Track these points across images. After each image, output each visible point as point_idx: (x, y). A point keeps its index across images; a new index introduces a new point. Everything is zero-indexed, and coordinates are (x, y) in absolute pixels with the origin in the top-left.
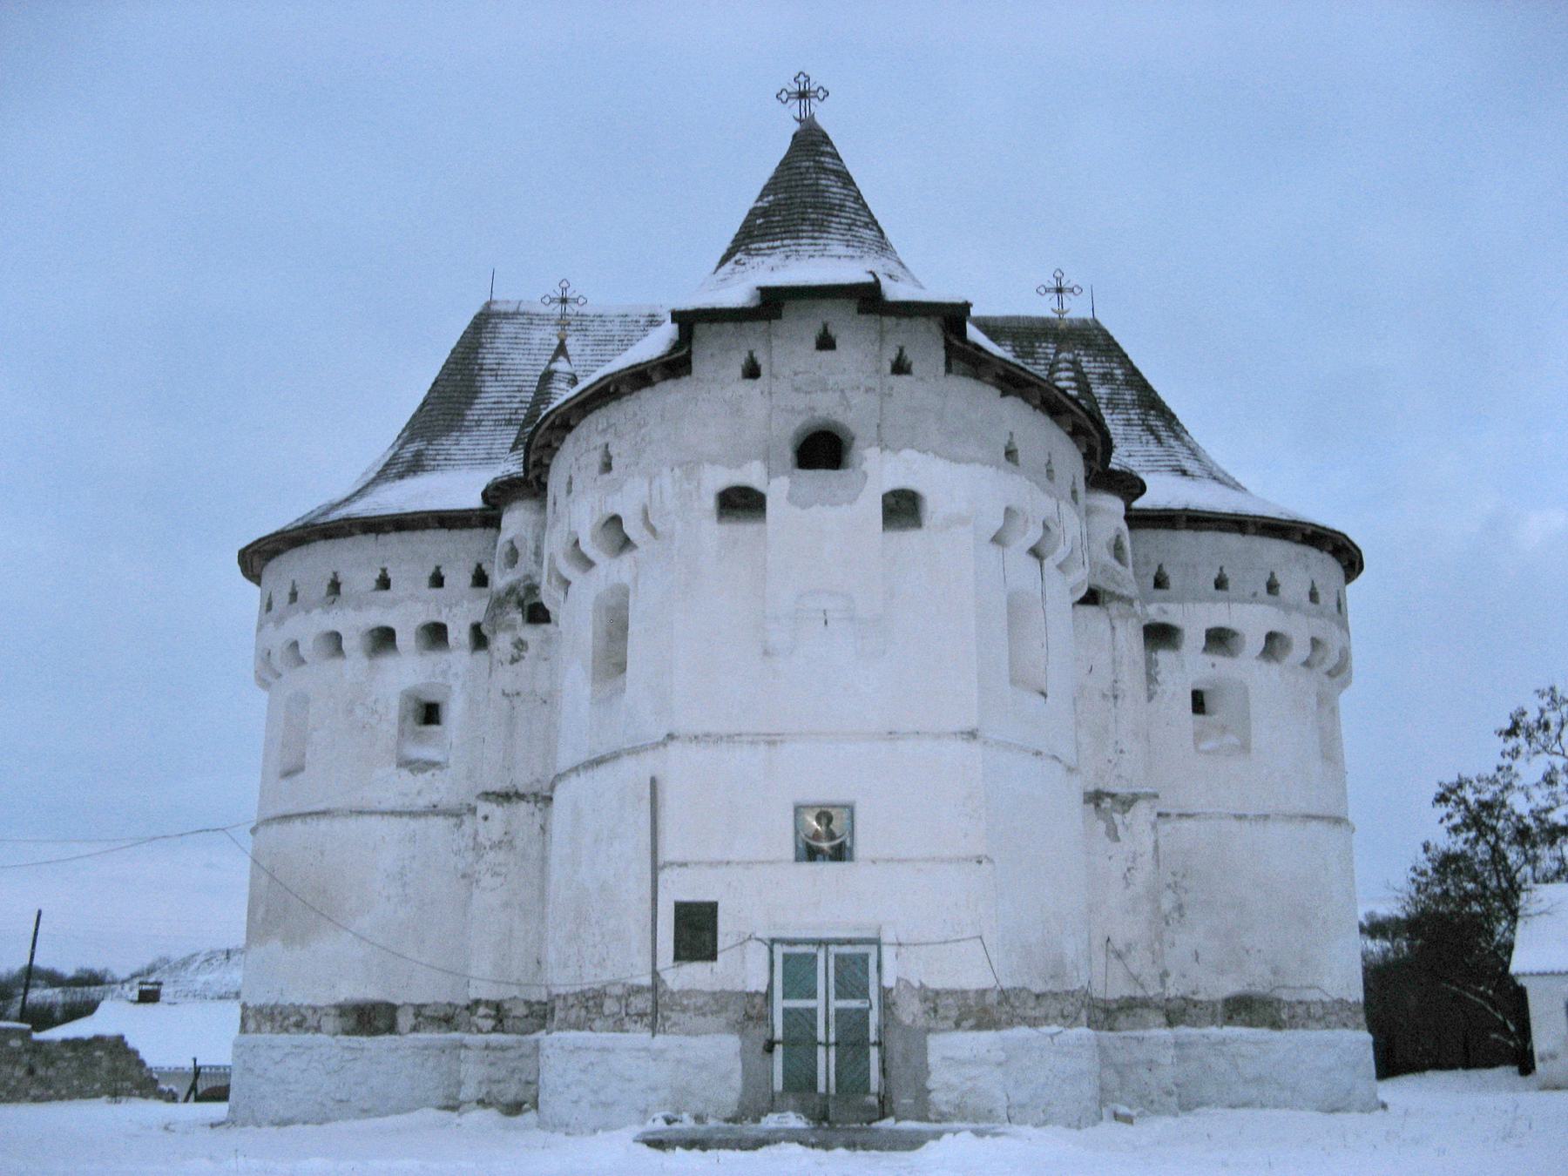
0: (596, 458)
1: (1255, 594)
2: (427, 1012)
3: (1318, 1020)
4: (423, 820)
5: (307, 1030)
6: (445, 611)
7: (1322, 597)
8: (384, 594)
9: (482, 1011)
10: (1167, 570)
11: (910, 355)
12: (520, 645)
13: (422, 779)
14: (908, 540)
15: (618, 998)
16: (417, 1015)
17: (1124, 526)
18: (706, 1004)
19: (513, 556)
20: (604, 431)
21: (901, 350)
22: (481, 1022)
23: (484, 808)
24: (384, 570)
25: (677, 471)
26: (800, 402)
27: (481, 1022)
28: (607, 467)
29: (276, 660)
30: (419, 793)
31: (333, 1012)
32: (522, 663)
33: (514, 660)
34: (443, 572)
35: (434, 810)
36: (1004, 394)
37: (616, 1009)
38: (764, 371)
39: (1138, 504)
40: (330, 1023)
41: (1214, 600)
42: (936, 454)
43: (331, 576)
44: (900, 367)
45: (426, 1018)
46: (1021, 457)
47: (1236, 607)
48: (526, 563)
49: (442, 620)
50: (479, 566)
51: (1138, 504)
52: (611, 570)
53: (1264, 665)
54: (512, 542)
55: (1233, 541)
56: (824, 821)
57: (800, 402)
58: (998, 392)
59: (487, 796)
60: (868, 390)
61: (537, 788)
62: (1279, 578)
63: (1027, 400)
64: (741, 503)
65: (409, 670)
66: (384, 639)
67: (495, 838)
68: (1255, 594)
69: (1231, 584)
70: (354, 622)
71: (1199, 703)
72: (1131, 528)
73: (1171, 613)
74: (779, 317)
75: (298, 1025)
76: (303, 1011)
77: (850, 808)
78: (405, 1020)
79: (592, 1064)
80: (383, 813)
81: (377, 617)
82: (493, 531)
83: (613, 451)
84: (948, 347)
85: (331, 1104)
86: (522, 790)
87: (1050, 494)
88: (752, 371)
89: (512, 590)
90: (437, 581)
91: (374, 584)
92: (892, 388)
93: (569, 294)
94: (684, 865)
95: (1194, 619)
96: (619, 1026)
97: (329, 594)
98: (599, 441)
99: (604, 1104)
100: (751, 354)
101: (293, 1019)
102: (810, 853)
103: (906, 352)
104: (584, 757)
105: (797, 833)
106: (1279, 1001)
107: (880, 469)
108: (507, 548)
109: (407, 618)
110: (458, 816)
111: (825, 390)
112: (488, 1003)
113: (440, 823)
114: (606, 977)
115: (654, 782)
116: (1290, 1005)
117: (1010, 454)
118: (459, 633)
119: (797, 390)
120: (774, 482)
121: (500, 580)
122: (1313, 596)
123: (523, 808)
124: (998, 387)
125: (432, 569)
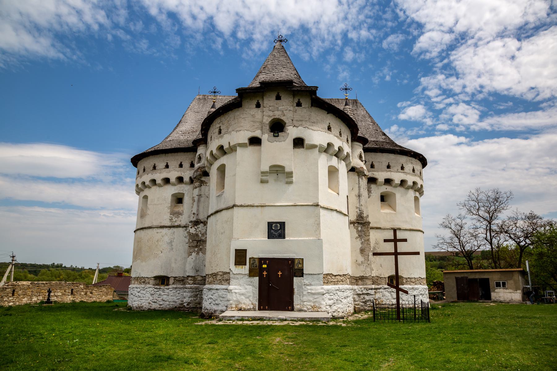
0: (217, 130)
2: (177, 279)
6: (183, 174)
7: (416, 171)
8: (167, 169)
9: (190, 278)
11: (301, 101)
14: (300, 151)
15: (221, 275)
17: (362, 151)
22: (190, 282)
26: (271, 113)
27: (190, 282)
28: (220, 132)
29: (140, 186)
39: (366, 146)
40: (152, 282)
41: (387, 171)
42: (308, 128)
44: (299, 104)
49: (182, 176)
50: (192, 162)
51: (366, 146)
55: (392, 156)
57: (271, 113)
60: (290, 110)
64: (255, 141)
66: (167, 181)
71: (383, 198)
75: (144, 282)
78: (171, 281)
81: (165, 175)
82: (195, 153)
83: (222, 128)
86: (202, 220)
87: (341, 140)
88: (258, 106)
90: (181, 166)
91: (164, 167)
93: (216, 90)
95: (381, 176)
96: (220, 283)
98: (218, 126)
99: (217, 304)
107: (292, 132)
109: (173, 175)
111: (278, 110)
112: (191, 277)
114: (218, 270)
116: (406, 279)
117: (329, 128)
118: (186, 179)
121: (197, 166)
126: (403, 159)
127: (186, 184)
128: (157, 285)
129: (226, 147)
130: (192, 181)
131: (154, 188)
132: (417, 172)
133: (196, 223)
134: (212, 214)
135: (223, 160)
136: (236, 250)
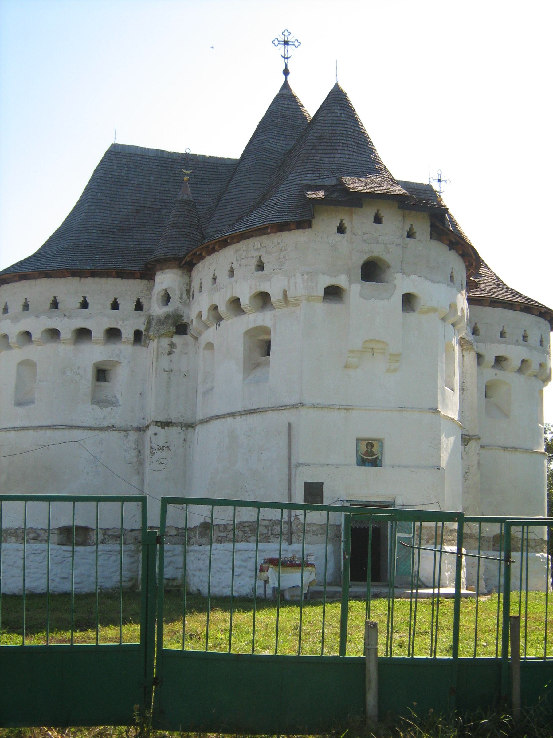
0: (254, 262)
1: (517, 341)
2: (110, 532)
3: (532, 548)
4: (106, 432)
5: (41, 541)
6: (120, 323)
10: (479, 326)
11: (415, 228)
12: (172, 345)
13: (106, 411)
14: (412, 316)
15: (266, 527)
16: (104, 534)
18: (317, 530)
19: (167, 298)
20: (258, 249)
21: (412, 225)
23: (153, 428)
24: (85, 298)
25: (305, 276)
28: (260, 267)
30: (104, 419)
31: (56, 532)
32: (173, 355)
33: (170, 353)
34: (119, 301)
35: (112, 427)
36: (450, 250)
37: (265, 531)
38: (348, 230)
40: (54, 538)
41: (500, 343)
42: (426, 278)
43: (53, 298)
44: (410, 235)
45: (109, 536)
46: (455, 278)
47: (509, 346)
48: (174, 305)
50: (139, 300)
52: (254, 319)
53: (518, 375)
54: (166, 290)
55: (509, 313)
56: (369, 447)
58: (449, 248)
59: (156, 423)
60: (397, 245)
61: (181, 420)
62: (528, 333)
63: (457, 252)
64: (333, 293)
65: (96, 352)
66: (83, 334)
67: (161, 445)
68: (517, 341)
69: (507, 335)
70: (67, 326)
72: (469, 304)
73: (482, 348)
74: (361, 206)
75: (35, 539)
76: (39, 532)
77: (380, 442)
79: (250, 557)
80: (84, 428)
82: (145, 282)
84: (433, 226)
85: (58, 579)
86: (173, 421)
88: (341, 230)
89: (167, 317)
90: (115, 306)
92: (407, 245)
94: (308, 465)
97: (51, 308)
98: (257, 254)
100: (342, 221)
101: (32, 535)
102: (362, 462)
103: (414, 227)
104: (238, 407)
105: (357, 452)
106: (517, 537)
107: (403, 283)
108: (163, 293)
109: (98, 325)
110: (126, 431)
113: (115, 435)
115: (289, 425)
117: (452, 276)
119: (365, 241)
120: (353, 286)
122: (525, 337)
123: (173, 431)
124: (449, 246)
125: (111, 300)
126: (527, 319)
127: (127, 343)
128: (63, 544)
129: (276, 296)
130: (138, 336)
131: (51, 347)
132: (533, 339)
133: (166, 424)
134: (233, 415)
135: (264, 319)
136: (306, 485)
